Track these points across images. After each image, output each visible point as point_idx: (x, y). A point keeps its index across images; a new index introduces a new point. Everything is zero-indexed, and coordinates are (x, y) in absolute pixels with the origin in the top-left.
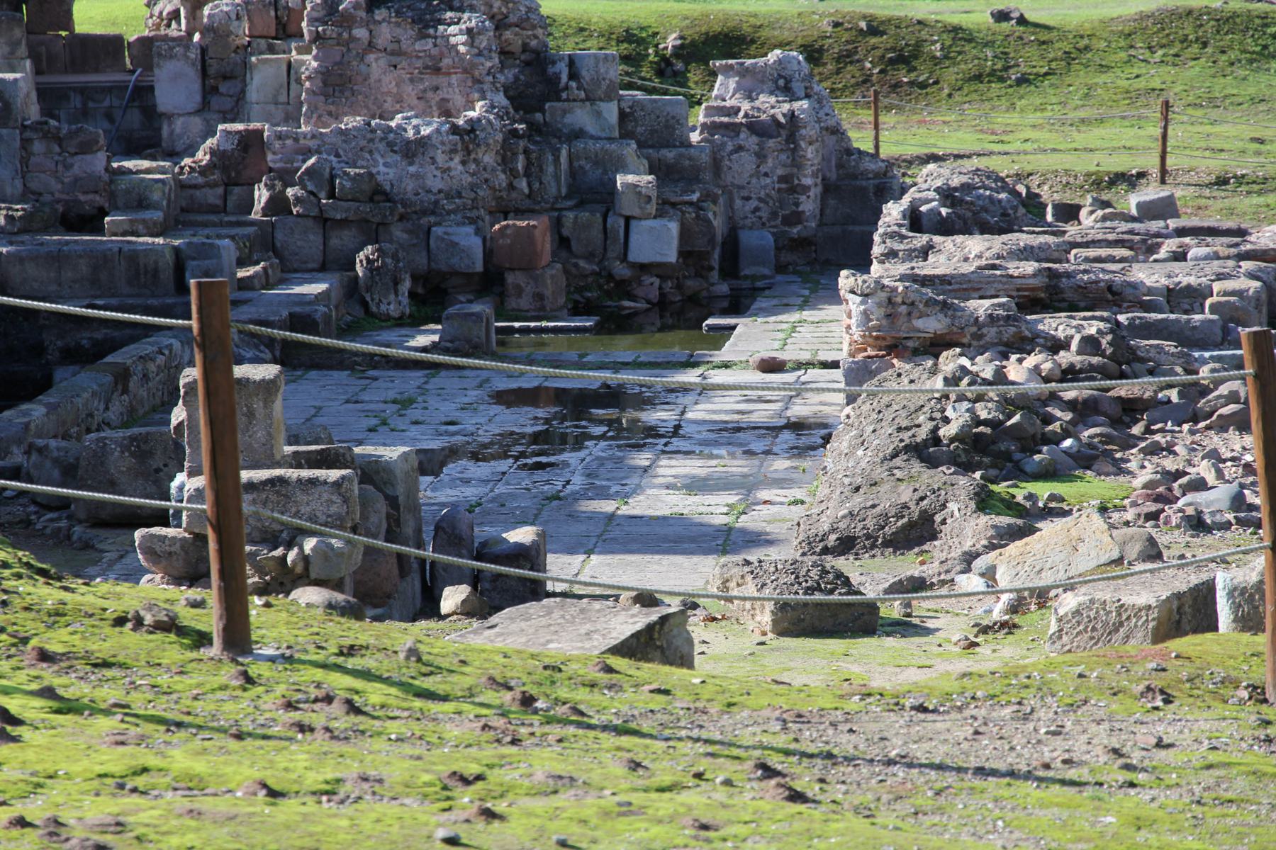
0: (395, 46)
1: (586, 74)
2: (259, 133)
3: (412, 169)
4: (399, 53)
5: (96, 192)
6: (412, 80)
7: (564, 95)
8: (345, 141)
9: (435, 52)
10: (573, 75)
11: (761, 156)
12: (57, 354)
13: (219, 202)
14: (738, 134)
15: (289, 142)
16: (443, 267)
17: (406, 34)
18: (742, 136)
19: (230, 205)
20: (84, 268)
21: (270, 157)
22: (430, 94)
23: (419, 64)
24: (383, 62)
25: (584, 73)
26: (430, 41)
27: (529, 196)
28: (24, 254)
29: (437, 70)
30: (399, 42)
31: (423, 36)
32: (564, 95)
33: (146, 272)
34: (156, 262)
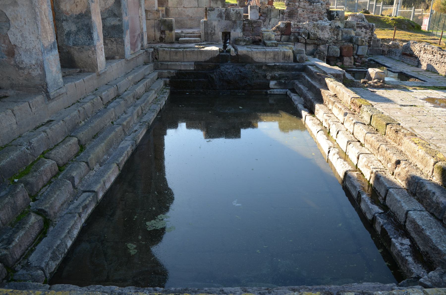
0: (304, 7)
1: (340, 15)
2: (290, 24)
3: (322, 33)
4: (305, 8)
5: (259, 36)
6: (307, 14)
7: (335, 19)
8: (308, 26)
9: (313, 8)
10: (337, 15)
11: (366, 33)
12: (270, 78)
13: (280, 39)
14: (362, 28)
15: (296, 26)
16: (331, 55)
17: (307, 4)
18: (363, 29)
19: (282, 39)
20: (272, 55)
21: (291, 29)
22: (311, 17)
23: (309, 11)
24: (301, 10)
25: (340, 14)
26: (312, 6)
27: (336, 40)
28: (257, 51)
29: (313, 12)
30: (305, 6)
31: (310, 5)
32: (335, 19)
33: (287, 57)
34: (290, 54)
